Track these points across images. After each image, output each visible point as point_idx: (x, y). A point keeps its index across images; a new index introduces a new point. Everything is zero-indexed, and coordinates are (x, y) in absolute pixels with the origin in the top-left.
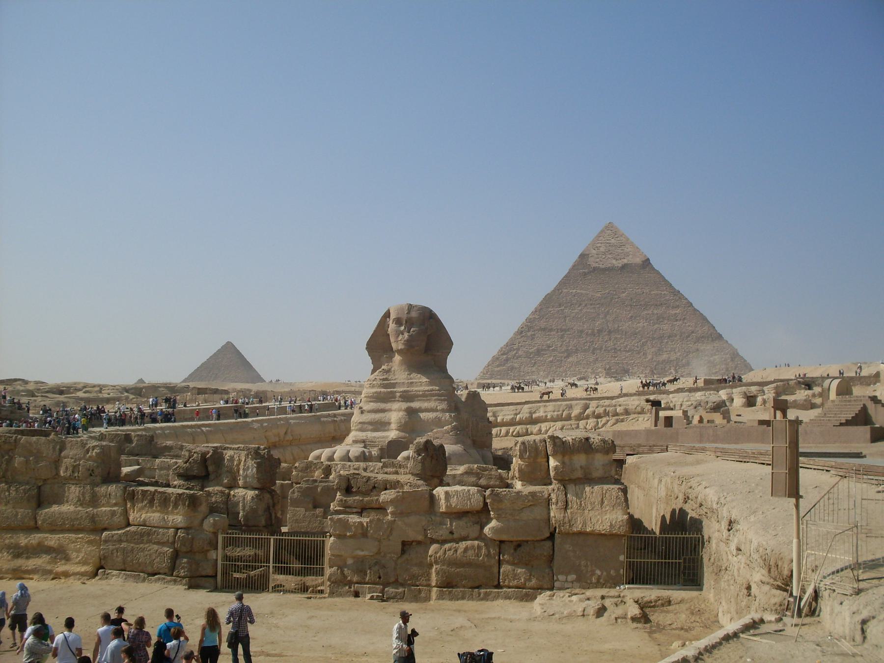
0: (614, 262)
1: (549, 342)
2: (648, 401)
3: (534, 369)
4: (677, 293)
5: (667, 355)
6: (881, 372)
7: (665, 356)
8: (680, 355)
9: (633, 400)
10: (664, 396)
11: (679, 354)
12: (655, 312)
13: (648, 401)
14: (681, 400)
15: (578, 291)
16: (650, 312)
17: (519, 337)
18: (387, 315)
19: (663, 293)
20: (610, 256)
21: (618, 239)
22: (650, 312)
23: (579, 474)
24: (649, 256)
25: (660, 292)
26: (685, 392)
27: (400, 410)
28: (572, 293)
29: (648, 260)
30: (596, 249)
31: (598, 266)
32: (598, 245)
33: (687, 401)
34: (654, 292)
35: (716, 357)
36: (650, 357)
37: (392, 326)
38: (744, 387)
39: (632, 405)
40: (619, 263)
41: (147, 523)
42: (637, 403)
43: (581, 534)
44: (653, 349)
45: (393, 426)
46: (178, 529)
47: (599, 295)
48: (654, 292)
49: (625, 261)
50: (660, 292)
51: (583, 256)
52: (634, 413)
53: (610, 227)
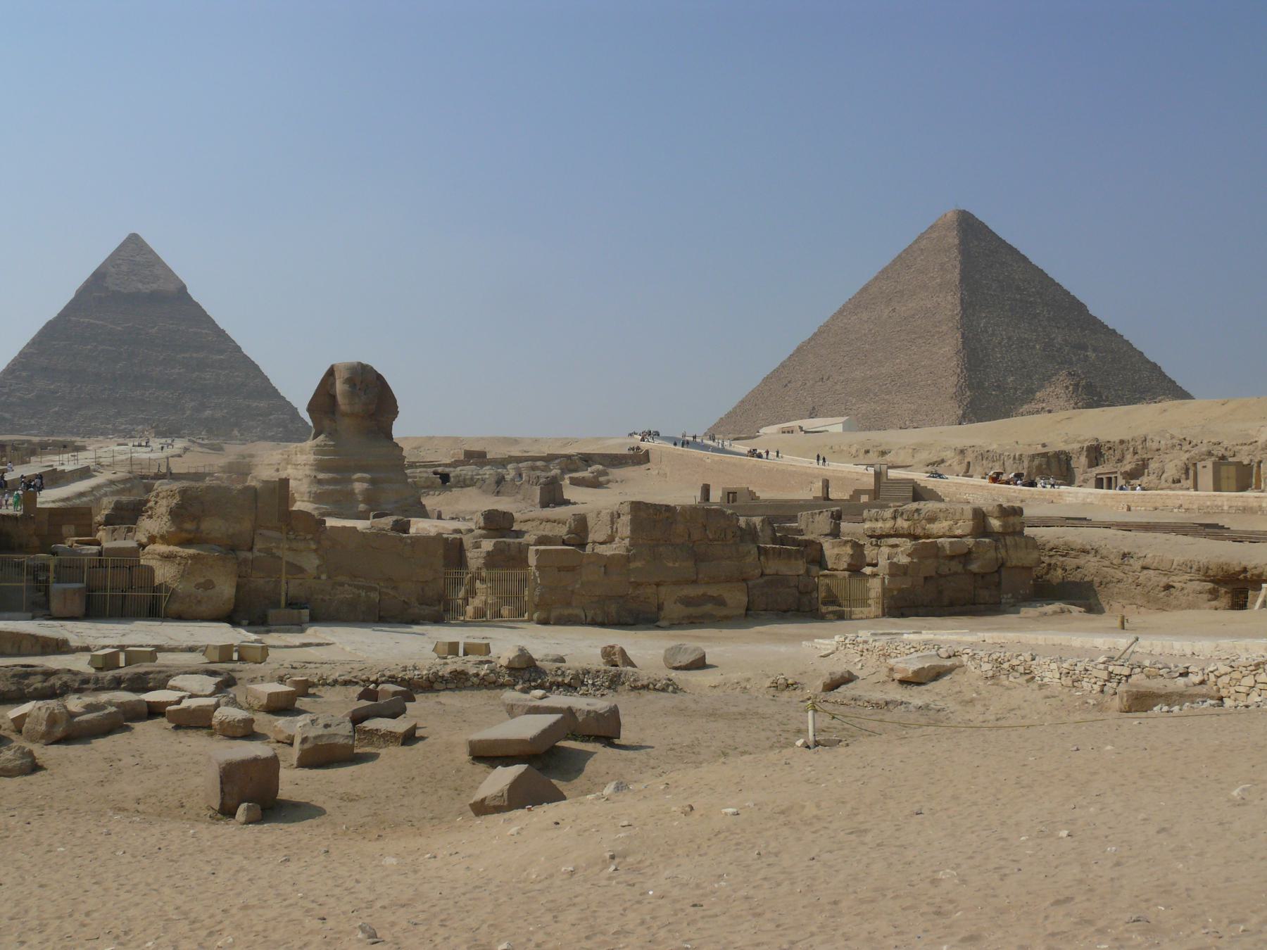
0: (140, 286)
1: (52, 387)
2: (435, 473)
3: (33, 422)
4: (221, 334)
5: (210, 412)
6: (650, 451)
7: (208, 413)
8: (227, 413)
9: (420, 472)
10: (452, 469)
11: (226, 411)
12: (195, 355)
13: (435, 473)
14: (470, 473)
15: (92, 321)
16: (187, 355)
17: (10, 377)
18: (331, 373)
19: (203, 331)
20: (135, 278)
21: (145, 256)
22: (187, 355)
23: (1011, 530)
24: (185, 282)
25: (199, 330)
26: (470, 465)
27: (361, 480)
28: (83, 322)
29: (183, 288)
30: (116, 267)
31: (119, 289)
32: (118, 262)
33: (476, 475)
34: (192, 330)
35: (272, 417)
36: (188, 413)
37: (340, 387)
38: (529, 462)
39: (420, 477)
40: (147, 289)
41: (780, 573)
42: (425, 475)
43: (1016, 567)
44: (193, 403)
45: (360, 498)
46: (798, 576)
47: (120, 328)
48: (192, 330)
49: (155, 286)
50: (199, 330)
51: (98, 277)
52: (424, 488)
53: (134, 240)
